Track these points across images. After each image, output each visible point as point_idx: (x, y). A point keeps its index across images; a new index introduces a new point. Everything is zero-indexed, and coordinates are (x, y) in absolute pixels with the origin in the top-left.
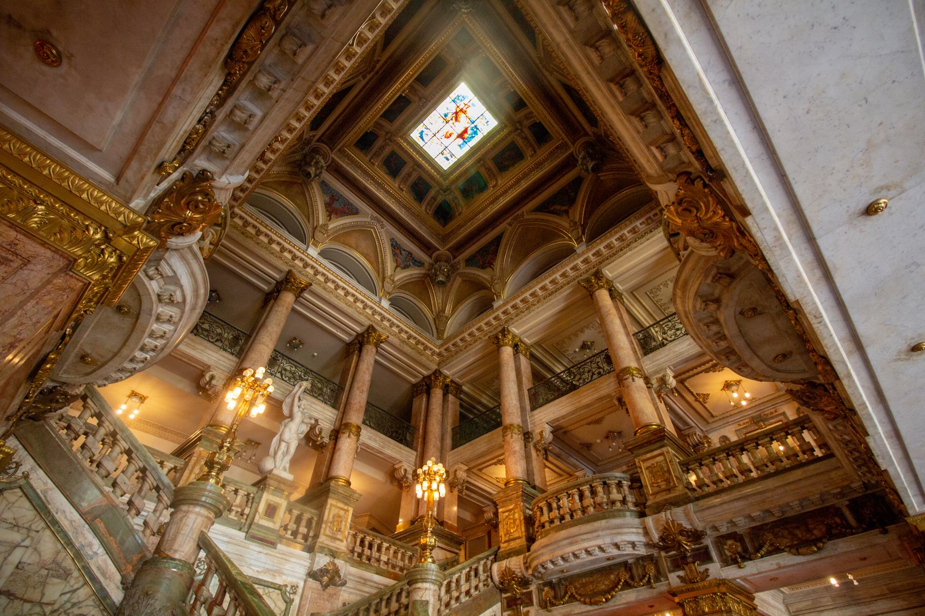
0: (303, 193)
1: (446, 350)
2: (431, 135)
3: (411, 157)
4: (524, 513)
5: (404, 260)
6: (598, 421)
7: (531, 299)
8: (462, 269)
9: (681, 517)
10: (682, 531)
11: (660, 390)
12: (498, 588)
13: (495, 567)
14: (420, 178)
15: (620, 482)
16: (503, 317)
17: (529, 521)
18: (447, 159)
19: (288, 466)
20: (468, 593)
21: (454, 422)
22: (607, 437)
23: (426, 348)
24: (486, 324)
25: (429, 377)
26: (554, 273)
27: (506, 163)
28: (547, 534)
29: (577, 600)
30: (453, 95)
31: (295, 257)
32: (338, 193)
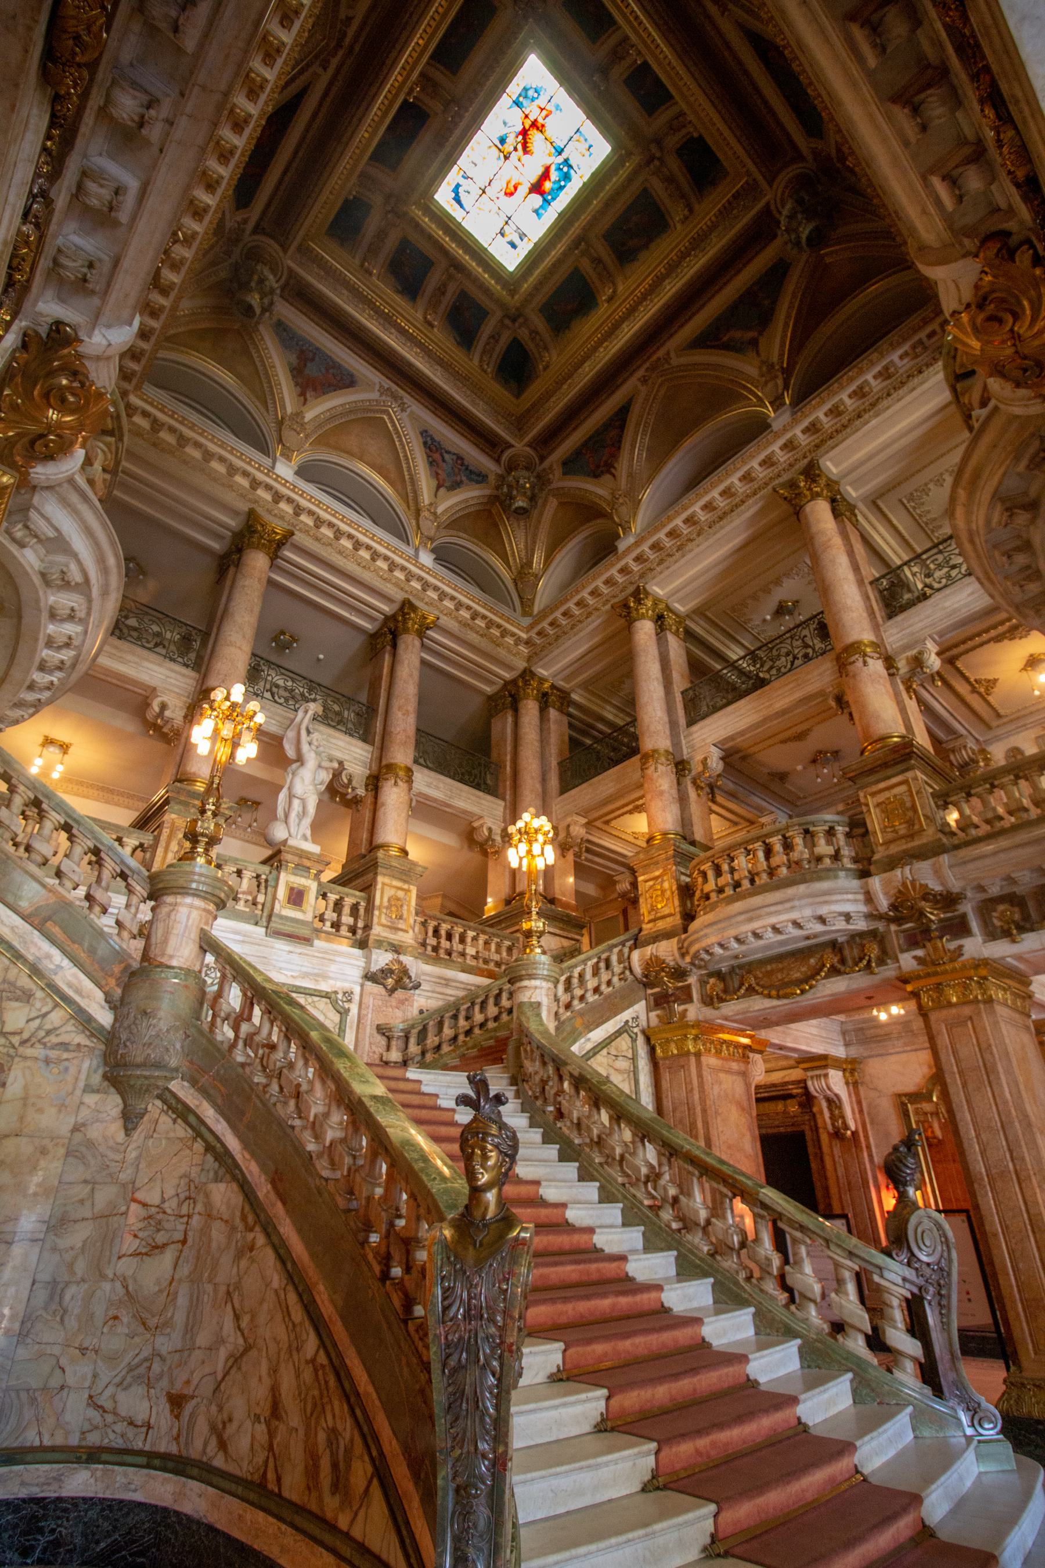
1: (539, 634)
4: (678, 880)
6: (800, 737)
7: (685, 530)
8: (560, 481)
9: (925, 874)
10: (927, 895)
11: (910, 676)
12: (640, 982)
13: (636, 955)
15: (832, 828)
16: (635, 567)
17: (686, 892)
18: (514, 246)
19: (309, 833)
20: (596, 990)
21: (561, 753)
22: (814, 761)
23: (505, 633)
24: (607, 582)
25: (514, 682)
28: (713, 907)
29: (757, 993)
31: (255, 484)
32: (311, 344)
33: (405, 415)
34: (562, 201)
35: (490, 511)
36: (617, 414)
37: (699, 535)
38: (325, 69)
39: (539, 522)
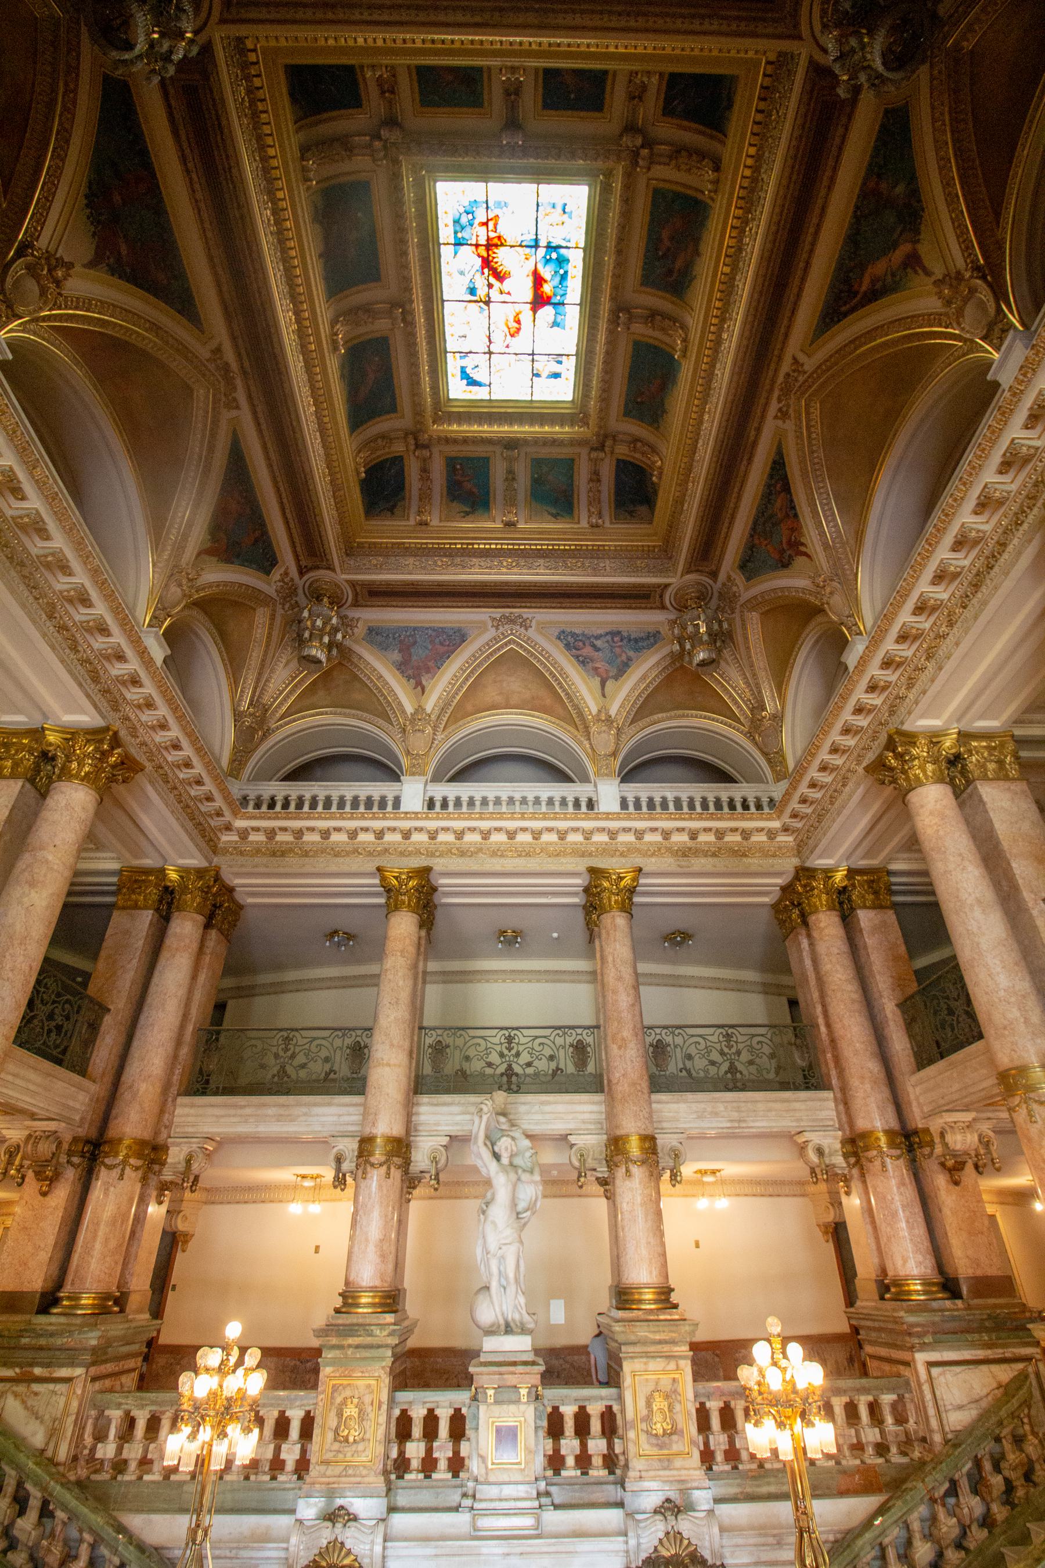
3: (489, 441)
5: (608, 657)
8: (747, 591)
14: (537, 463)
18: (556, 375)
23: (746, 834)
26: (976, 470)
27: (679, 264)
30: (446, 233)
33: (531, 633)
34: (574, 290)
35: (682, 666)
36: (771, 476)
37: (951, 624)
38: (238, 407)
39: (748, 648)
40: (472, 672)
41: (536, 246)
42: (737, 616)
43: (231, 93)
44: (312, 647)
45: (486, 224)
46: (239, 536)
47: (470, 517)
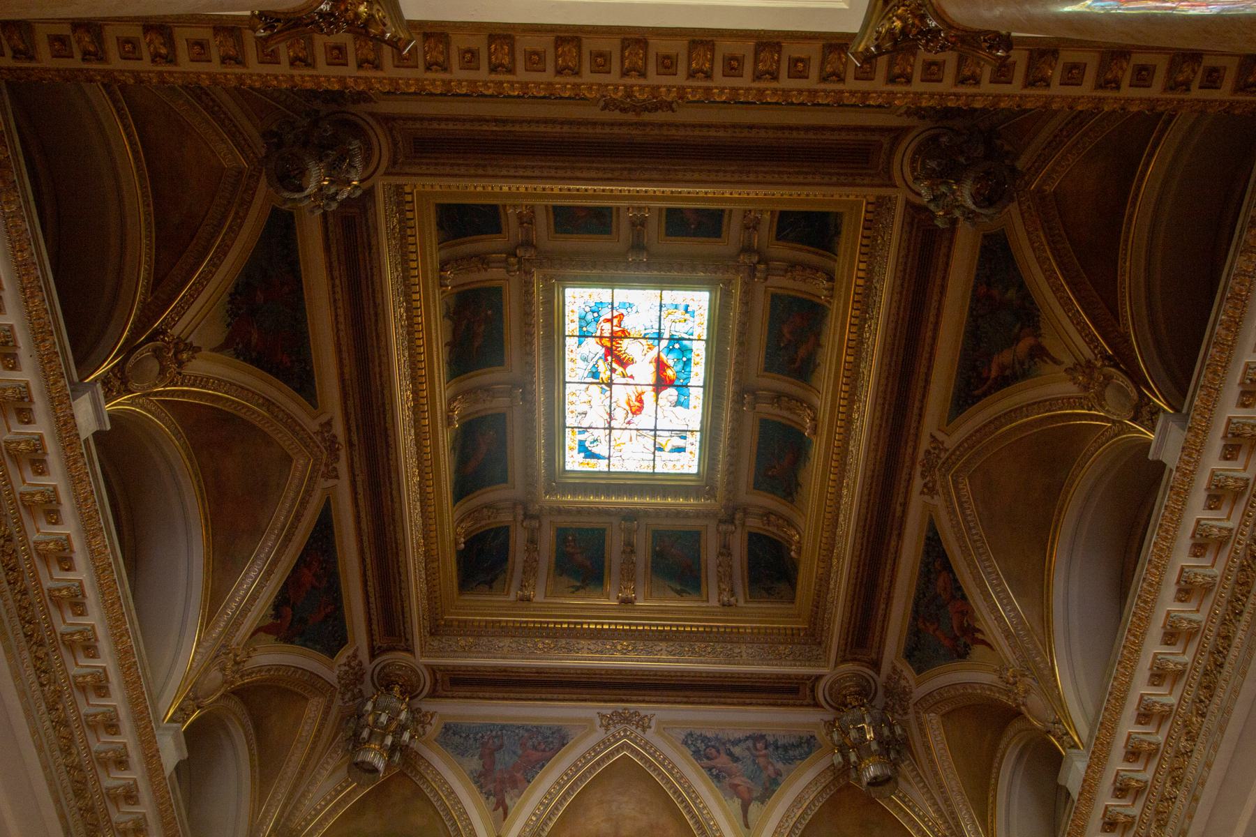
0: (418, 792)
2: (602, 434)
3: (607, 513)
8: (919, 686)
14: (658, 536)
18: (680, 450)
30: (571, 327)
33: (650, 735)
34: (698, 374)
35: (849, 786)
36: (927, 553)
38: (337, 477)
39: (932, 761)
40: (571, 788)
41: (659, 338)
42: (911, 716)
43: (384, 217)
44: (370, 750)
45: (611, 321)
46: (306, 610)
47: (580, 593)
